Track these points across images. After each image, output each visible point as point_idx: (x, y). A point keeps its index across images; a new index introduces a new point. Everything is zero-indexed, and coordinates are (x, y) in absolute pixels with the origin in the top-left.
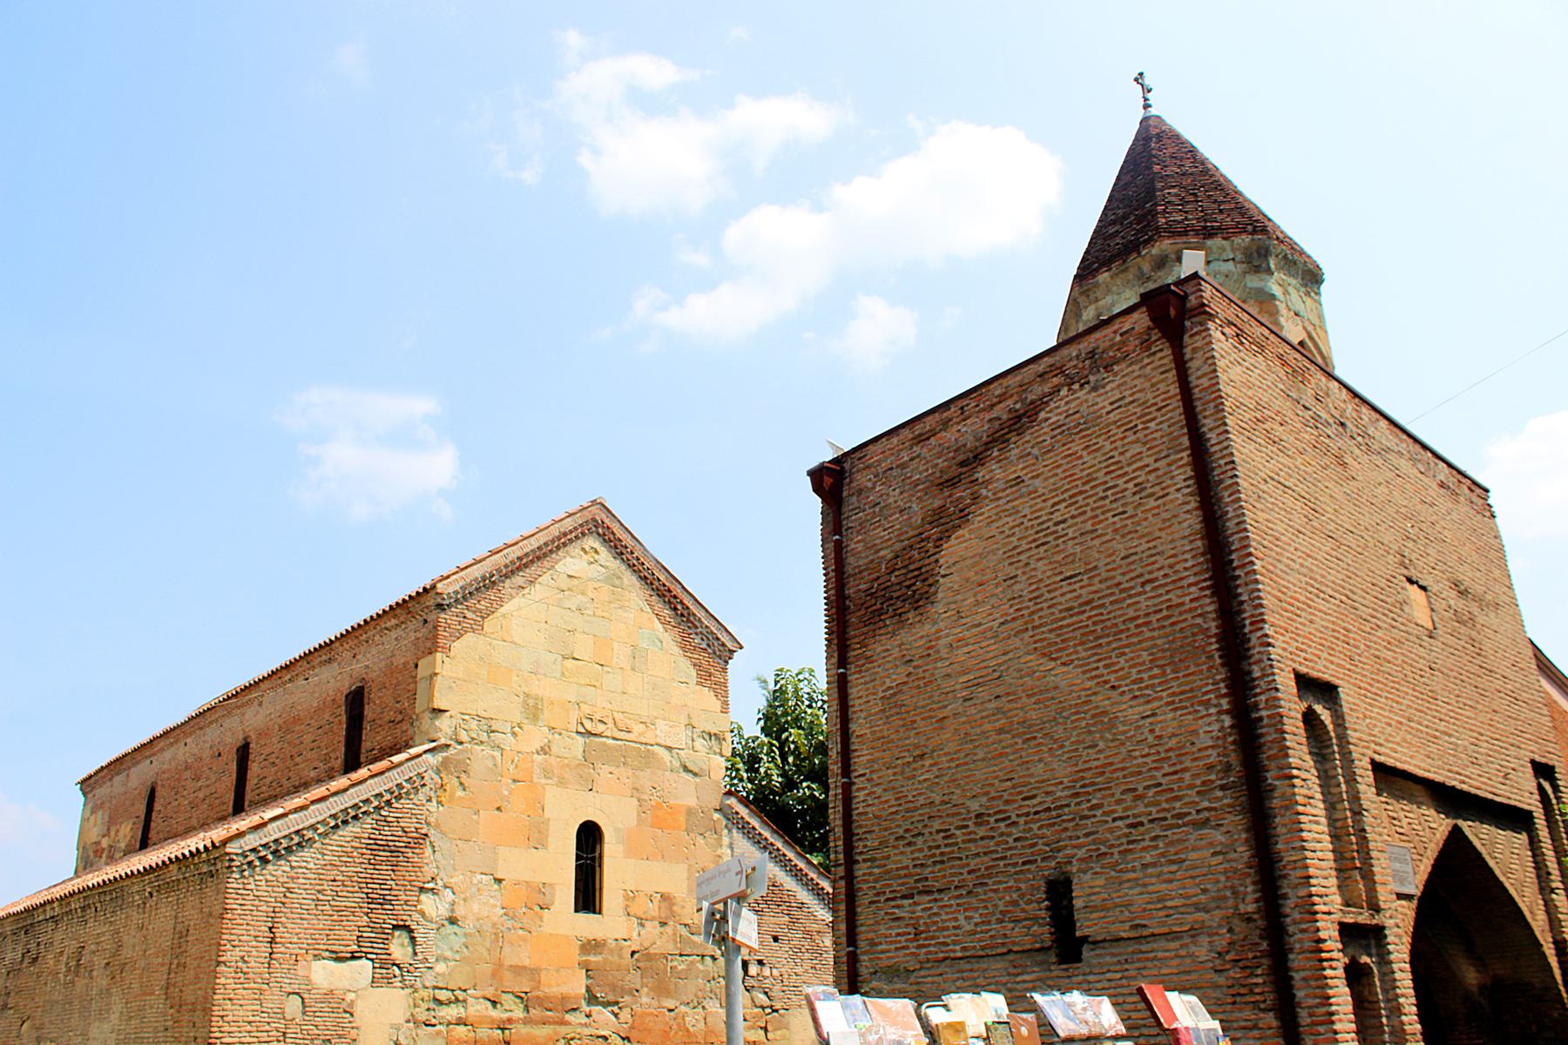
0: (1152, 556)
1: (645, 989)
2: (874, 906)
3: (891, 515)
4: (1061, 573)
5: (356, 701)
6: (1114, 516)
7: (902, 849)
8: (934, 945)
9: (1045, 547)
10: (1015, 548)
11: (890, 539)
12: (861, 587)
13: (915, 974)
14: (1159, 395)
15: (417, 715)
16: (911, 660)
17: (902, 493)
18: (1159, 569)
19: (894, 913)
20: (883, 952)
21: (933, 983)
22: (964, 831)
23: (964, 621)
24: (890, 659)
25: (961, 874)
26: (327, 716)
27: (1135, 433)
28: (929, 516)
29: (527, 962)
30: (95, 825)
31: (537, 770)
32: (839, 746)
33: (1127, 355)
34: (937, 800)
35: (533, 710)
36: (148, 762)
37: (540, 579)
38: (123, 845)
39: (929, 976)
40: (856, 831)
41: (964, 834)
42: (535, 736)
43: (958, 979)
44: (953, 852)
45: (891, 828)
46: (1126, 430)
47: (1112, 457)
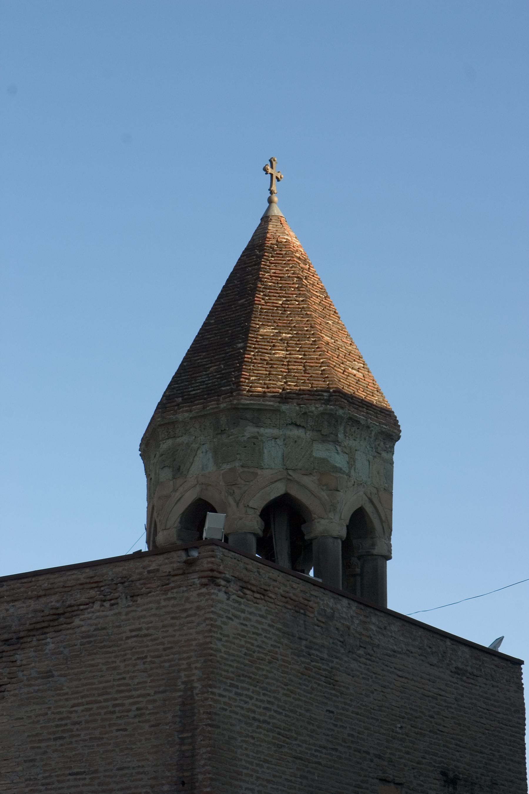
0: (139, 773)
4: (70, 768)
6: (118, 730)
9: (61, 742)
10: (37, 735)
14: (167, 637)
18: (143, 786)
27: (144, 663)
33: (150, 592)
46: (138, 658)
47: (124, 678)
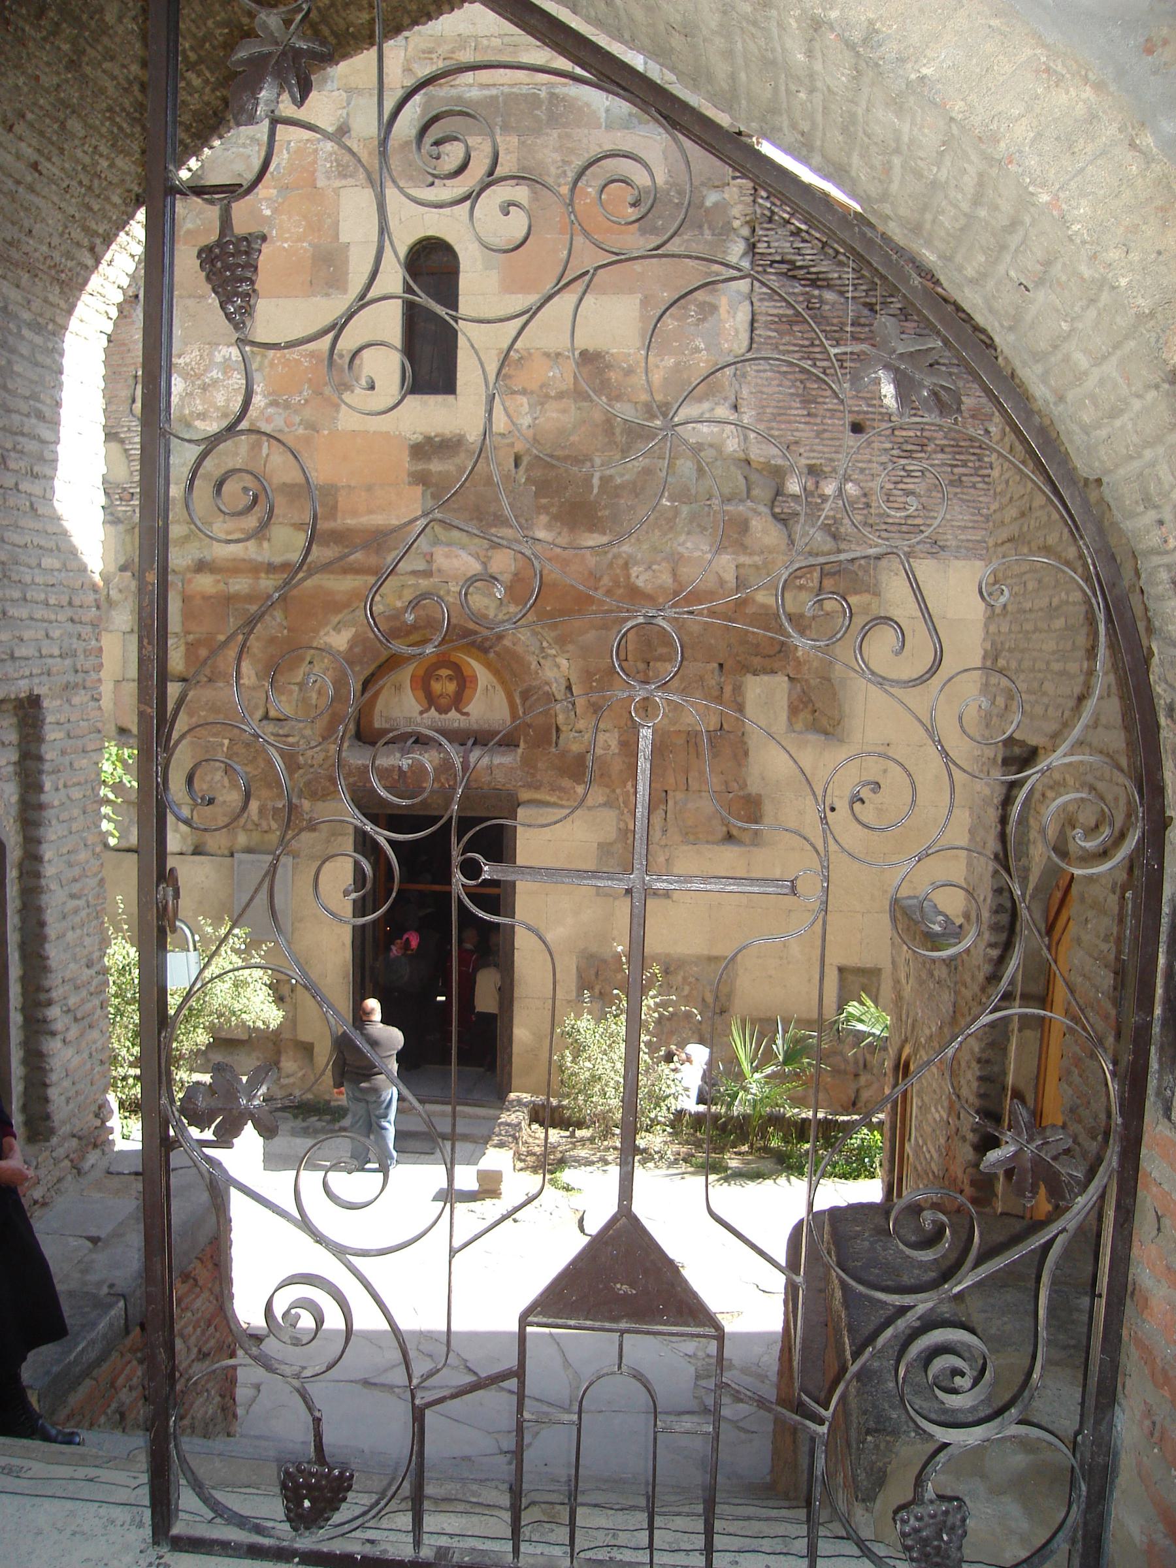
1: (544, 519)
31: (324, 166)
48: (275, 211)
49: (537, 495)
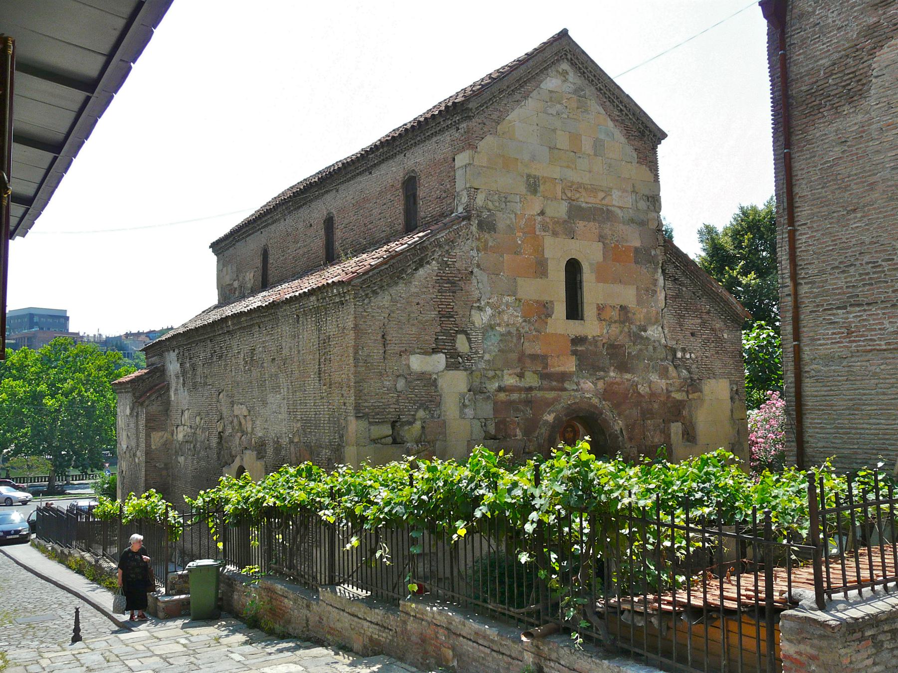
1: (613, 368)
2: (814, 314)
3: (830, 32)
5: (410, 184)
7: (837, 275)
8: (863, 341)
11: (829, 50)
12: (802, 88)
13: (846, 360)
15: (458, 193)
16: (846, 141)
17: (839, 14)
19: (831, 319)
20: (821, 345)
21: (861, 366)
22: (890, 262)
23: (893, 110)
24: (826, 141)
25: (888, 293)
26: (389, 197)
28: (864, 31)
29: (539, 352)
30: (227, 274)
31: (538, 226)
32: (785, 204)
34: (867, 241)
35: (533, 185)
36: (259, 232)
37: (531, 95)
38: (249, 286)
39: (858, 361)
40: (800, 263)
41: (889, 265)
42: (535, 205)
43: (882, 364)
44: (880, 277)
45: (828, 261)
48: (522, 242)
49: (610, 359)
